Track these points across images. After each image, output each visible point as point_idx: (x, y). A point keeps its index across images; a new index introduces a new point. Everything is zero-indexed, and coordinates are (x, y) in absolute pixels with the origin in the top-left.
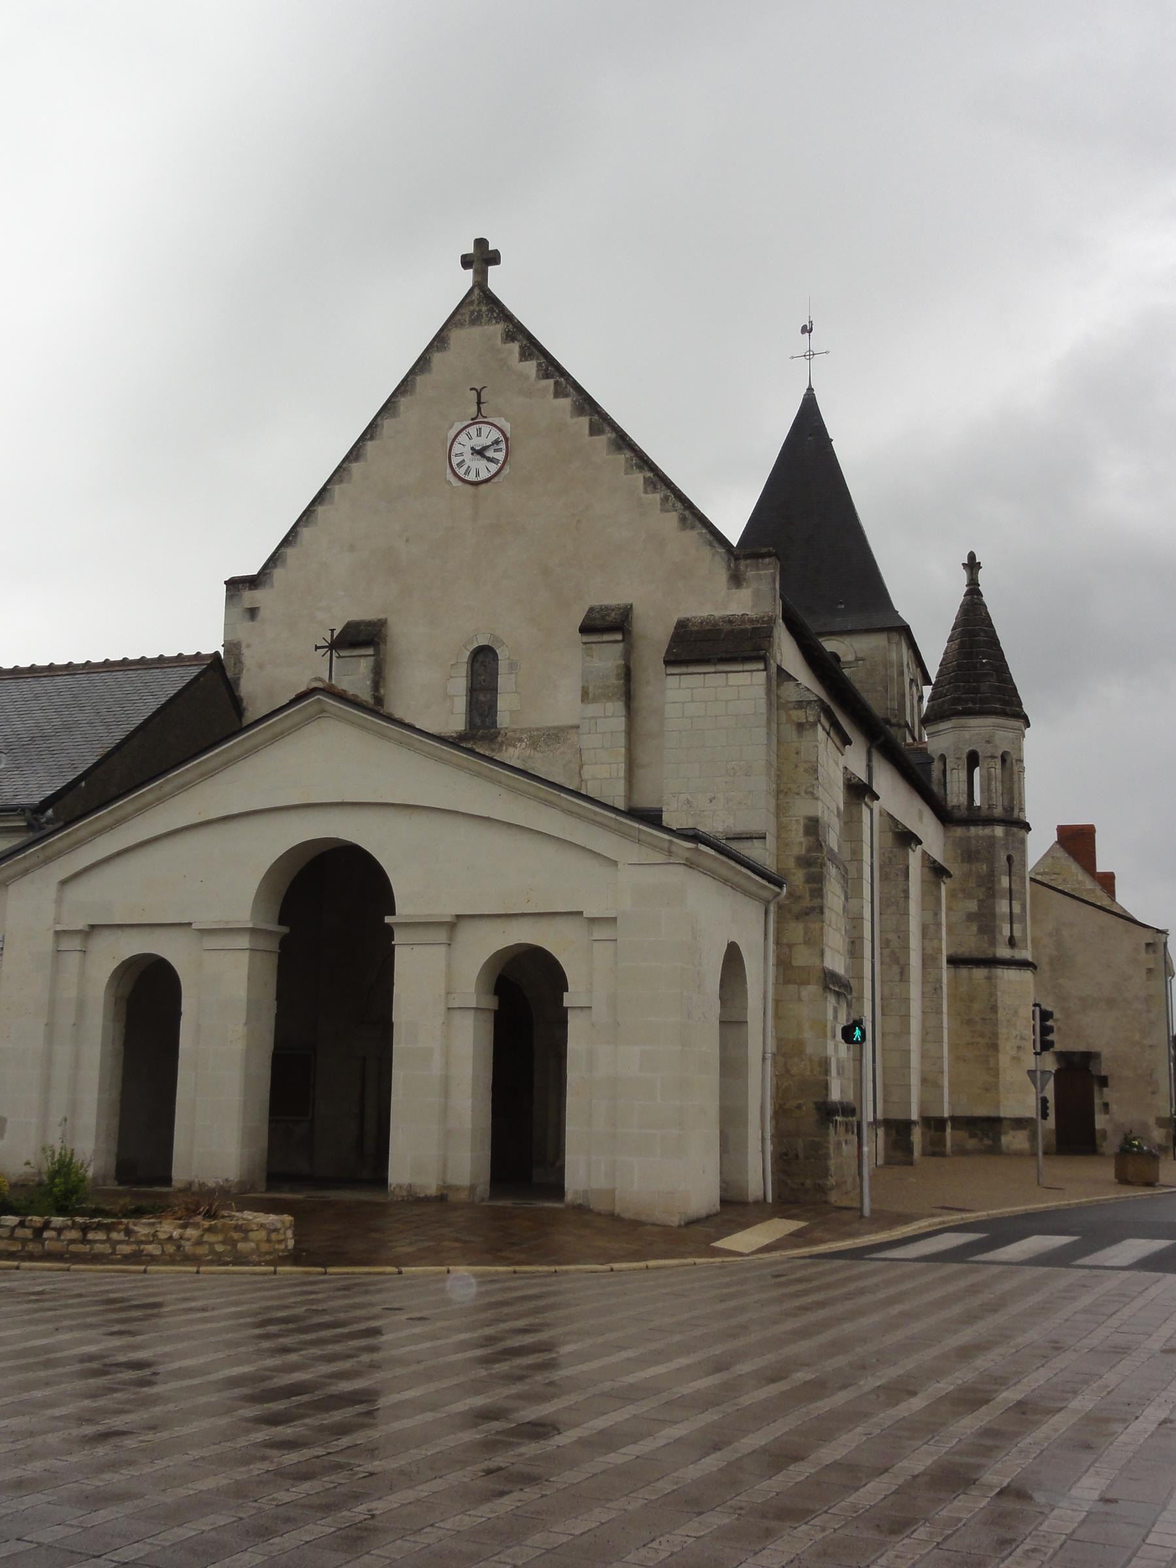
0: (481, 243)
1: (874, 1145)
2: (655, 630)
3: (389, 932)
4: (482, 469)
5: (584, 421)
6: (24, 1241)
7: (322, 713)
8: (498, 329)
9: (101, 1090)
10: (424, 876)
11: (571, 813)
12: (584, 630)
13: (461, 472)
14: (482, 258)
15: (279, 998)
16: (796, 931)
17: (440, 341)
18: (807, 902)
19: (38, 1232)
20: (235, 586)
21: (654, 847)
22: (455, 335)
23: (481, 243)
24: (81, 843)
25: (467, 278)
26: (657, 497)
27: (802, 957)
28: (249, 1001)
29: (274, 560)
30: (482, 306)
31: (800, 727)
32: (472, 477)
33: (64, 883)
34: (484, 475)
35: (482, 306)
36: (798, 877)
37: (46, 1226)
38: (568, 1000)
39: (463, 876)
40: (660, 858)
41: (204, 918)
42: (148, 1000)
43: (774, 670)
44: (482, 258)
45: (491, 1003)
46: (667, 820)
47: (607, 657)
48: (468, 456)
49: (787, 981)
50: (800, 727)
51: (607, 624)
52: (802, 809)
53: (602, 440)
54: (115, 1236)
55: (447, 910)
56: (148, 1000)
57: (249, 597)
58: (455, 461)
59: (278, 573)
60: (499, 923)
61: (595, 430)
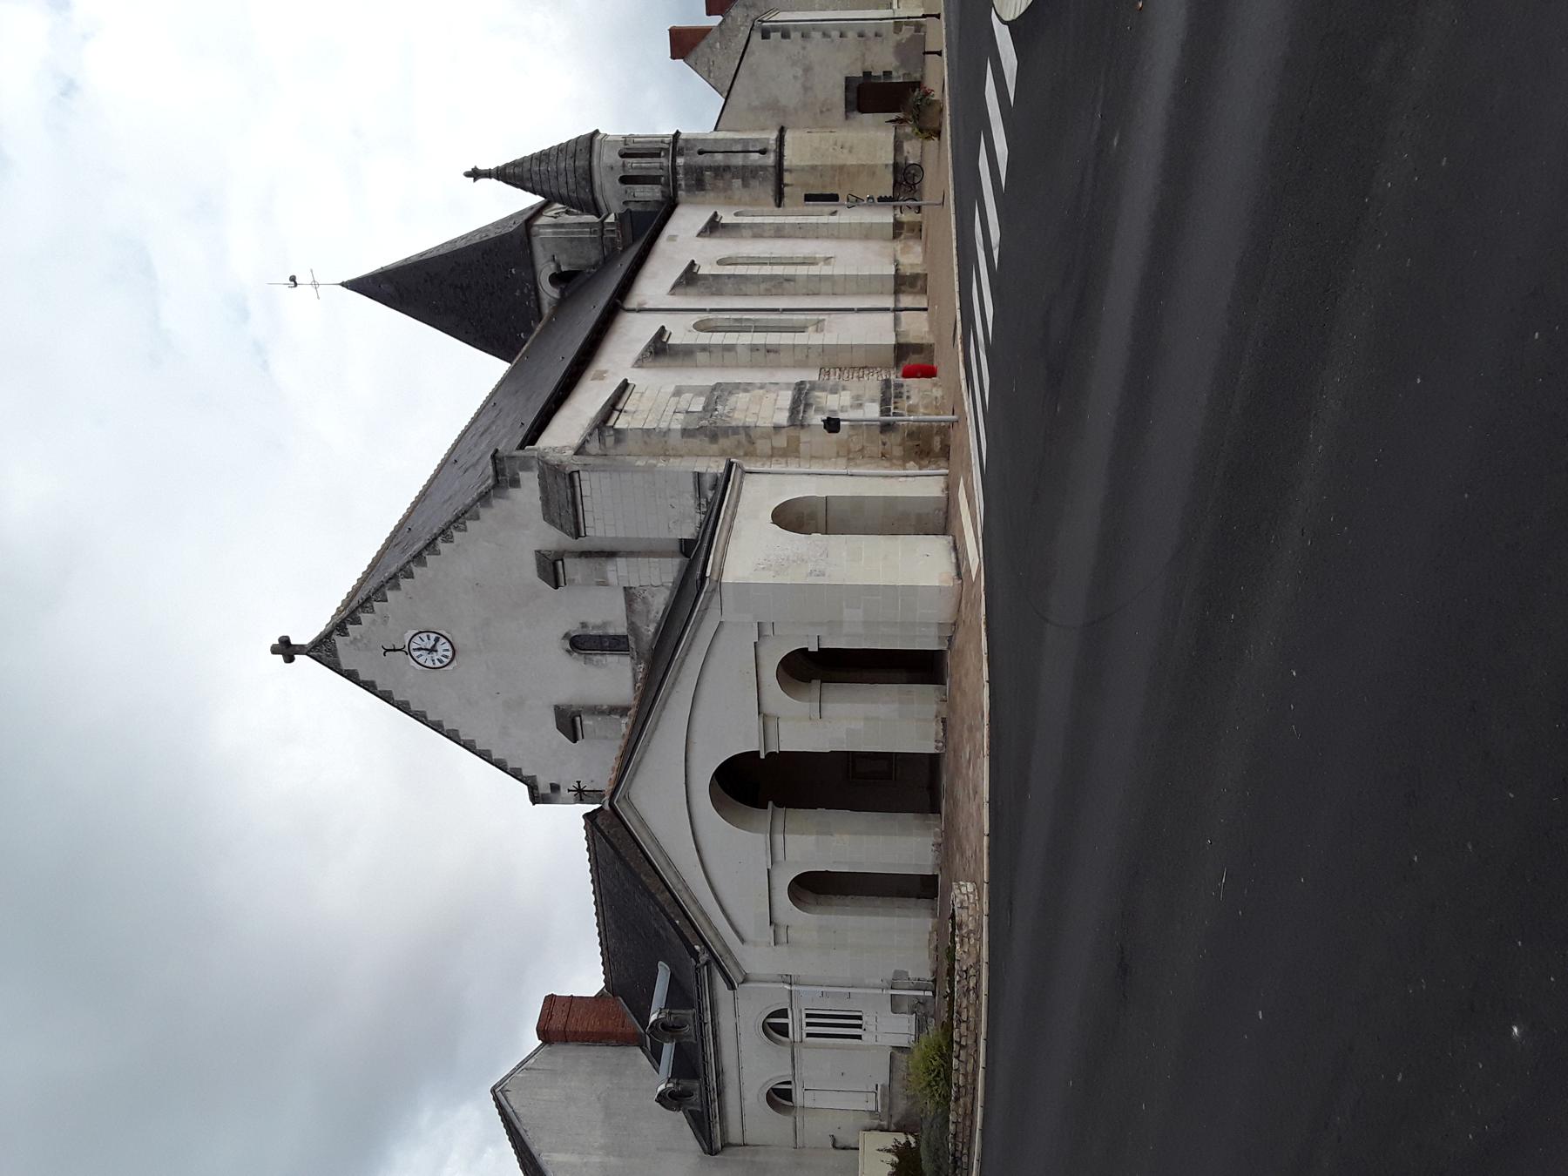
0: (274, 650)
1: (916, 388)
2: (553, 538)
3: (770, 755)
4: (443, 646)
5: (404, 583)
6: (968, 1055)
7: (626, 798)
8: (339, 641)
9: (877, 914)
10: (731, 731)
11: (689, 650)
12: (557, 587)
13: (446, 661)
14: (286, 650)
15: (812, 805)
16: (763, 446)
17: (351, 676)
18: (742, 437)
19: (962, 1047)
20: (536, 798)
21: (710, 600)
22: (344, 667)
23: (274, 650)
24: (717, 934)
25: (300, 659)
26: (455, 534)
27: (781, 441)
28: (818, 833)
29: (516, 774)
30: (323, 650)
31: (618, 441)
32: (450, 654)
33: (743, 941)
34: (447, 646)
35: (323, 650)
36: (724, 443)
37: (959, 1043)
38: (813, 648)
39: (730, 705)
40: (716, 598)
41: (765, 862)
42: (814, 887)
43: (579, 460)
44: (286, 650)
45: (816, 683)
46: (688, 531)
47: (574, 569)
48: (436, 656)
49: (797, 451)
50: (618, 441)
51: (551, 569)
52: (675, 439)
53: (416, 570)
54: (965, 1004)
55: (755, 722)
56: (814, 887)
57: (544, 788)
58: (438, 664)
59: (525, 773)
60: (763, 690)
61: (410, 575)
